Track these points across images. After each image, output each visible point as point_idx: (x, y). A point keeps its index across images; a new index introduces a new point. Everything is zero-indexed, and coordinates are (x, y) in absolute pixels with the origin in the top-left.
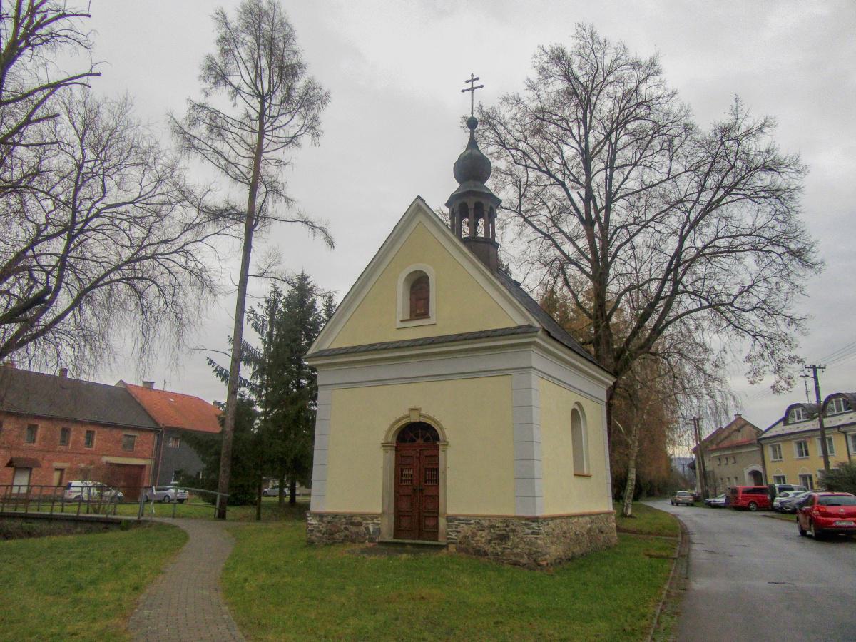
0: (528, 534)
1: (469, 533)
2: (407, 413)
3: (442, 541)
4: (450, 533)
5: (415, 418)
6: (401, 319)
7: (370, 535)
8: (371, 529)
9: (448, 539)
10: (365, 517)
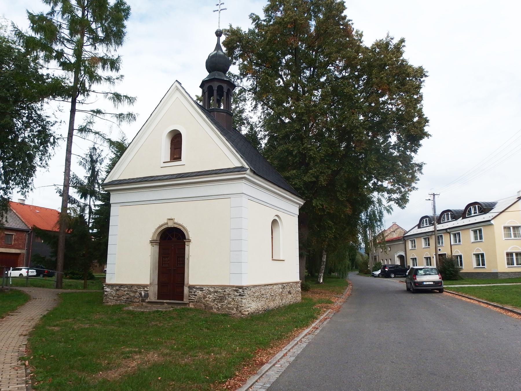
0: (237, 296)
1: (202, 296)
2: (166, 221)
3: (186, 300)
4: (191, 296)
5: (171, 225)
6: (164, 161)
7: (142, 297)
8: (143, 294)
9: (190, 299)
10: (139, 286)
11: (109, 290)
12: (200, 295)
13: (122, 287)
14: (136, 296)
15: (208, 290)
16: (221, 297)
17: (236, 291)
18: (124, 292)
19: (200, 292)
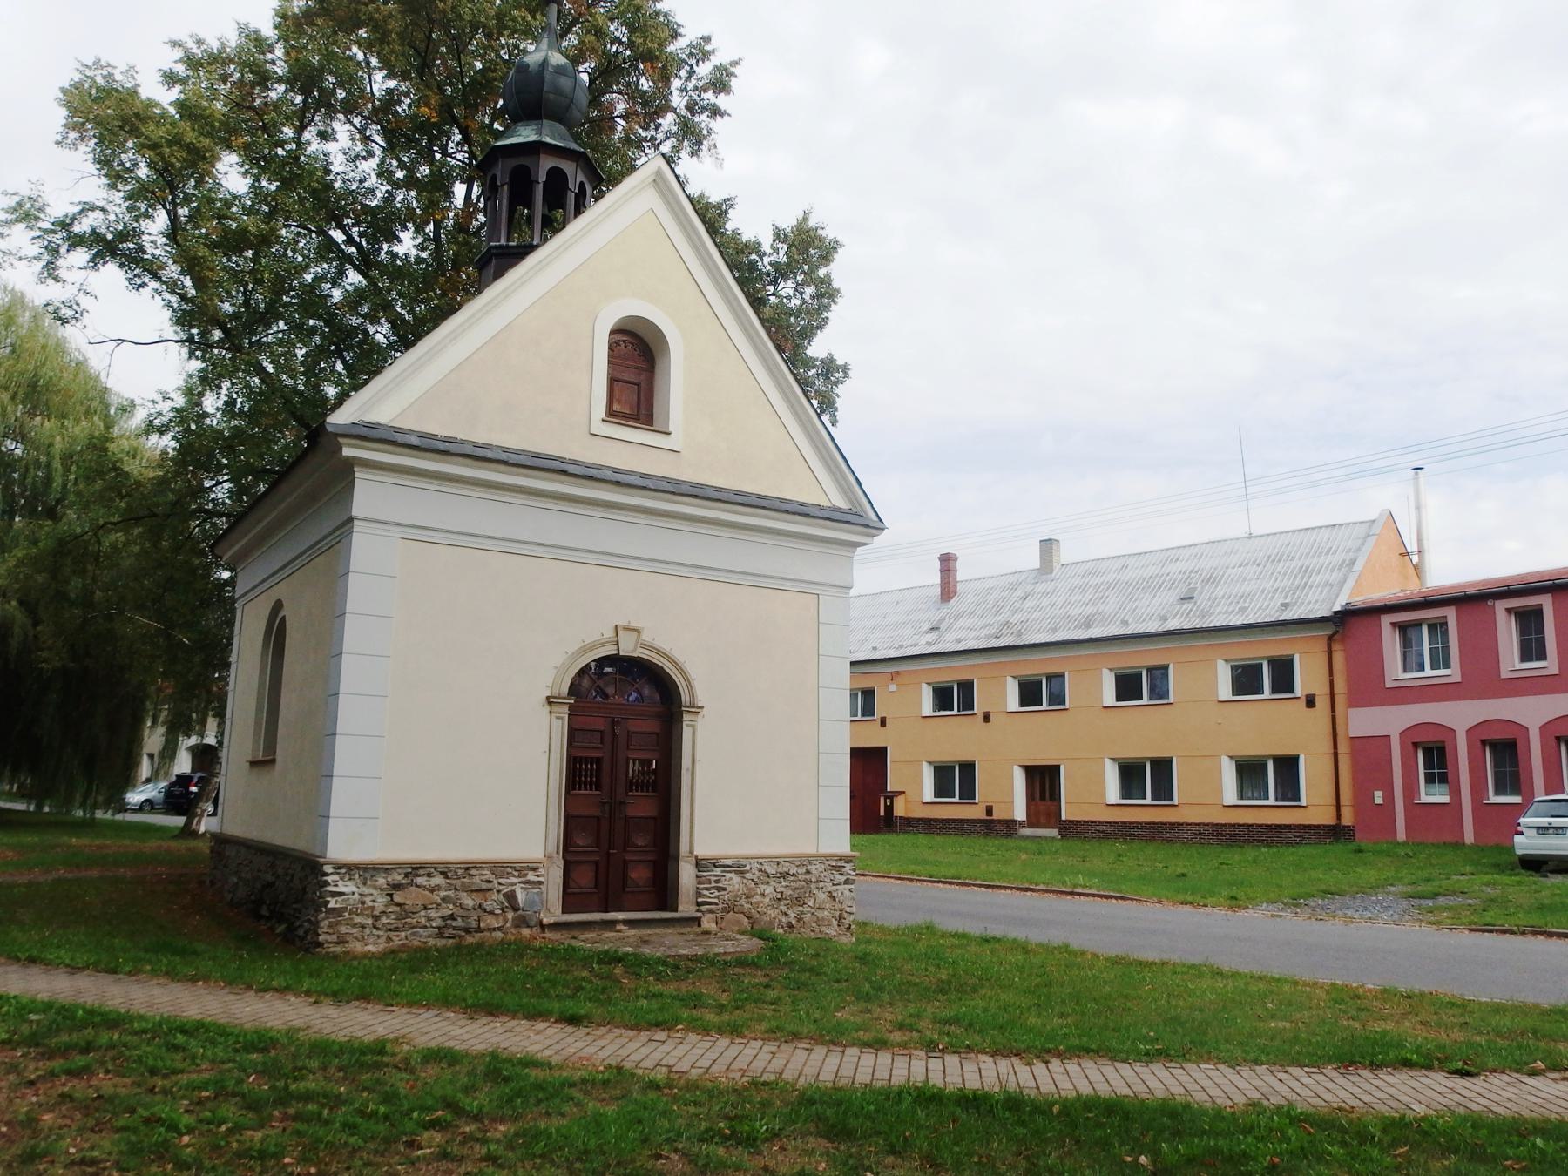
3: (686, 908)
4: (705, 892)
5: (628, 648)
8: (521, 896)
10: (502, 868)
11: (355, 889)
12: (737, 886)
13: (421, 872)
14: (489, 905)
15: (760, 870)
16: (796, 889)
17: (838, 868)
18: (432, 891)
19: (736, 879)
